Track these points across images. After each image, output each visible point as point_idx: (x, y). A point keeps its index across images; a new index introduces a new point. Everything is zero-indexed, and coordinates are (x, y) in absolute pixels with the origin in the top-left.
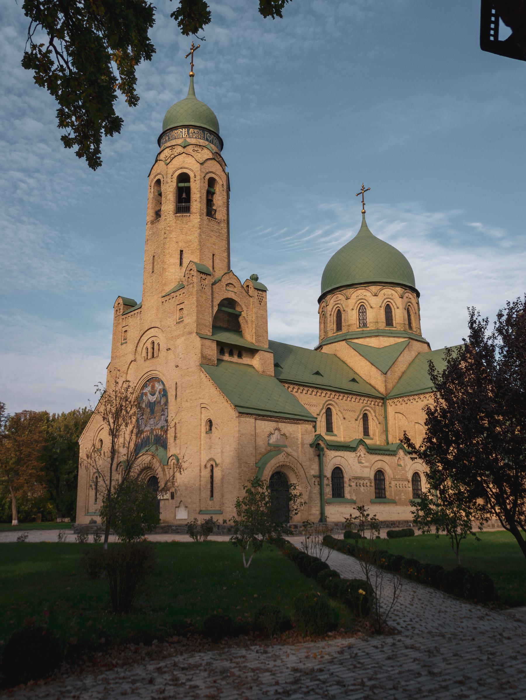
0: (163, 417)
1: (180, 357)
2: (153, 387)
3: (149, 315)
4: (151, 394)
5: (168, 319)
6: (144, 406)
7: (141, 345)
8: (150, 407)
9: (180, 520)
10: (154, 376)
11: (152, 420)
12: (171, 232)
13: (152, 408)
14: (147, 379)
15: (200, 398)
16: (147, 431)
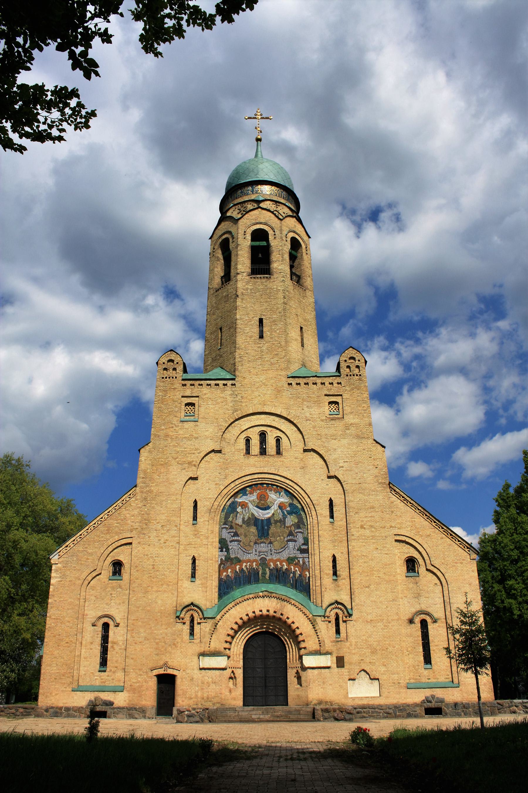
0: (291, 544)
1: (341, 465)
2: (262, 497)
3: (256, 393)
4: (257, 507)
5: (306, 409)
6: (239, 521)
7: (235, 430)
8: (255, 525)
9: (361, 698)
10: (267, 482)
11: (262, 545)
12: (290, 298)
13: (263, 527)
14: (250, 484)
15: (391, 527)
16: (249, 561)
